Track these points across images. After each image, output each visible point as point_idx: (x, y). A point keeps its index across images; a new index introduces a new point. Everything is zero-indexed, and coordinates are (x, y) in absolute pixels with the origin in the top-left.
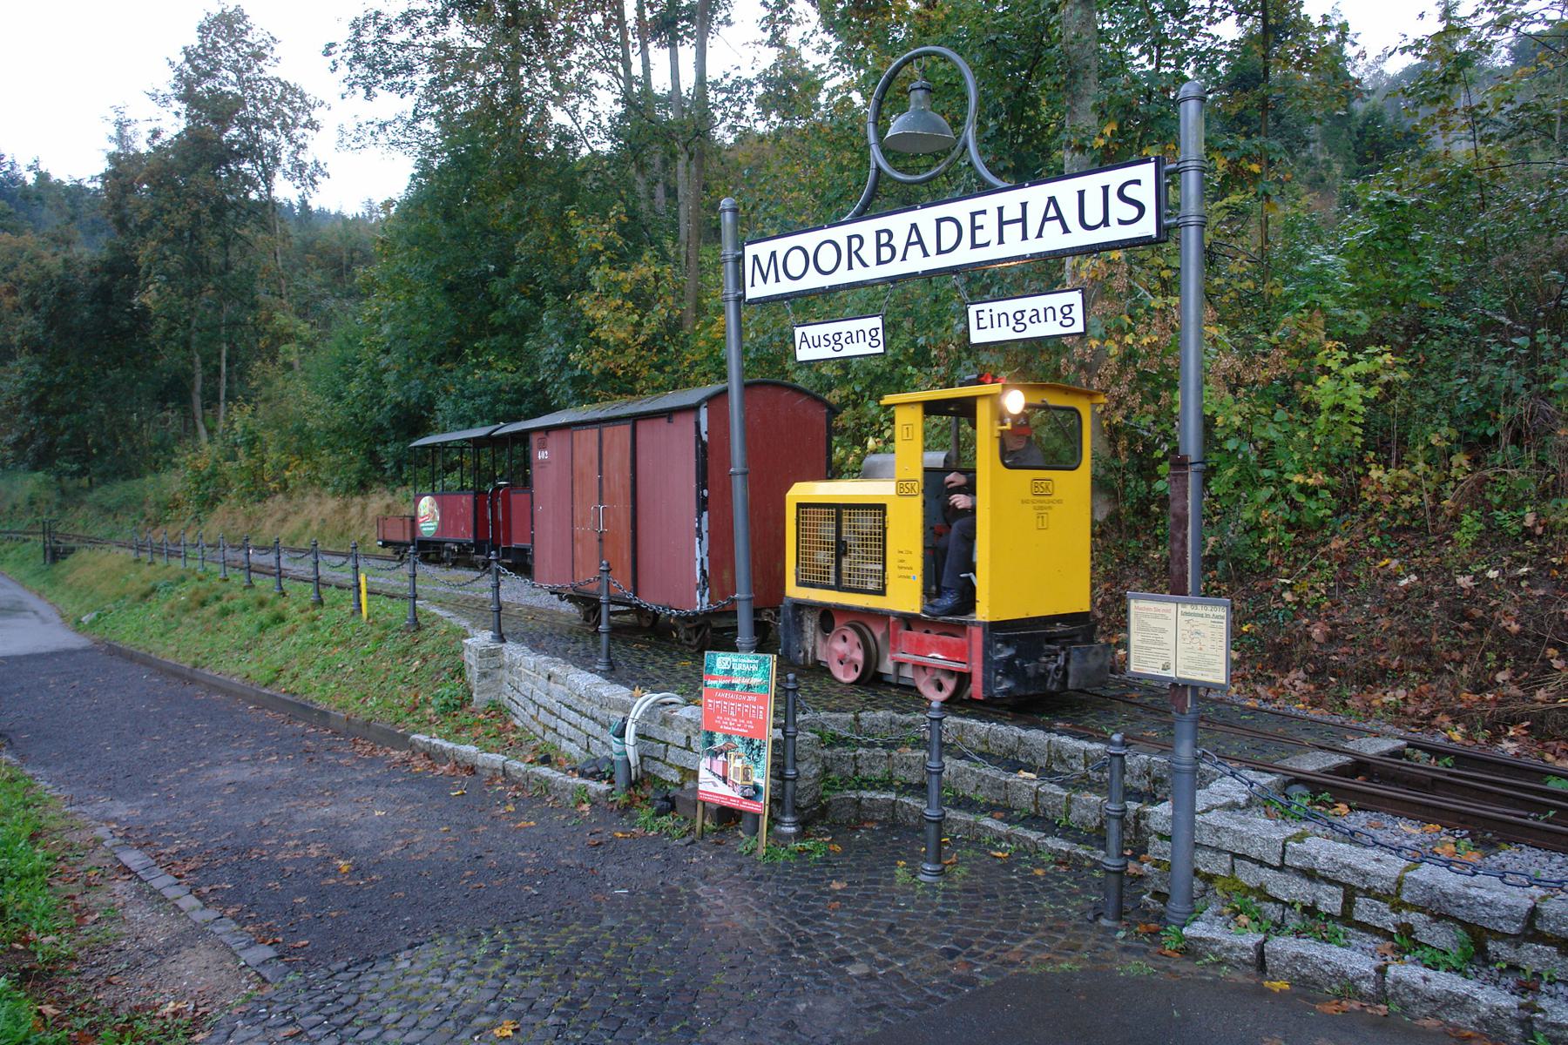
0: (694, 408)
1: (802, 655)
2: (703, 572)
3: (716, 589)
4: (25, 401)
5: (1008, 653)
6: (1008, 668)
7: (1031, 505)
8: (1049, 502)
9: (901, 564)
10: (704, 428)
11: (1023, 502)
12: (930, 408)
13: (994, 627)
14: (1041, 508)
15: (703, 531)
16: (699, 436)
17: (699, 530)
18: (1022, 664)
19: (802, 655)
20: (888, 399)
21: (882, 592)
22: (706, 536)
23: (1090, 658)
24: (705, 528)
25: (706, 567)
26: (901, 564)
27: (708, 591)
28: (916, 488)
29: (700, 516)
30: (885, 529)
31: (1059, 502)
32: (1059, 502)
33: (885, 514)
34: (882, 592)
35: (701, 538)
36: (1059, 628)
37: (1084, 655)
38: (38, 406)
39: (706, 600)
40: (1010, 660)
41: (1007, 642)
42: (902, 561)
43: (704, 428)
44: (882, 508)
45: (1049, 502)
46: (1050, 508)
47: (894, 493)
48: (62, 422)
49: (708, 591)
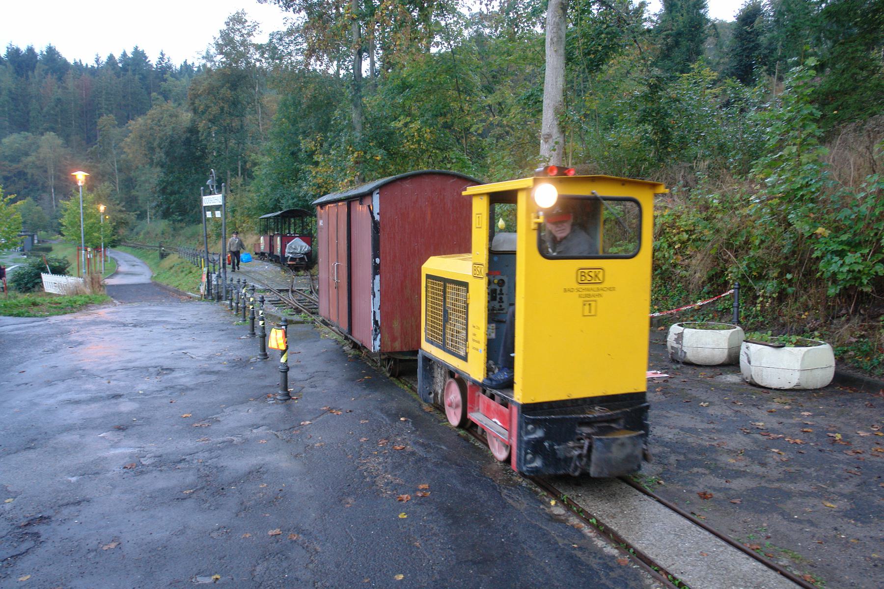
0: (370, 194)
1: (432, 395)
2: (376, 322)
3: (386, 336)
4: (158, 189)
5: (539, 434)
6: (536, 447)
8: (598, 289)
9: (475, 338)
10: (376, 210)
11: (565, 290)
13: (527, 409)
15: (376, 290)
16: (373, 217)
17: (373, 288)
18: (551, 446)
19: (432, 395)
21: (465, 358)
22: (378, 294)
23: (614, 449)
24: (377, 287)
25: (378, 318)
27: (379, 336)
29: (374, 279)
30: (468, 305)
31: (612, 289)
32: (612, 289)
33: (468, 292)
34: (465, 358)
35: (374, 296)
36: (597, 412)
37: (607, 446)
38: (163, 191)
39: (378, 343)
40: (539, 442)
41: (537, 424)
42: (474, 335)
43: (376, 210)
44: (465, 285)
45: (598, 289)
46: (600, 295)
48: (172, 198)
49: (379, 336)
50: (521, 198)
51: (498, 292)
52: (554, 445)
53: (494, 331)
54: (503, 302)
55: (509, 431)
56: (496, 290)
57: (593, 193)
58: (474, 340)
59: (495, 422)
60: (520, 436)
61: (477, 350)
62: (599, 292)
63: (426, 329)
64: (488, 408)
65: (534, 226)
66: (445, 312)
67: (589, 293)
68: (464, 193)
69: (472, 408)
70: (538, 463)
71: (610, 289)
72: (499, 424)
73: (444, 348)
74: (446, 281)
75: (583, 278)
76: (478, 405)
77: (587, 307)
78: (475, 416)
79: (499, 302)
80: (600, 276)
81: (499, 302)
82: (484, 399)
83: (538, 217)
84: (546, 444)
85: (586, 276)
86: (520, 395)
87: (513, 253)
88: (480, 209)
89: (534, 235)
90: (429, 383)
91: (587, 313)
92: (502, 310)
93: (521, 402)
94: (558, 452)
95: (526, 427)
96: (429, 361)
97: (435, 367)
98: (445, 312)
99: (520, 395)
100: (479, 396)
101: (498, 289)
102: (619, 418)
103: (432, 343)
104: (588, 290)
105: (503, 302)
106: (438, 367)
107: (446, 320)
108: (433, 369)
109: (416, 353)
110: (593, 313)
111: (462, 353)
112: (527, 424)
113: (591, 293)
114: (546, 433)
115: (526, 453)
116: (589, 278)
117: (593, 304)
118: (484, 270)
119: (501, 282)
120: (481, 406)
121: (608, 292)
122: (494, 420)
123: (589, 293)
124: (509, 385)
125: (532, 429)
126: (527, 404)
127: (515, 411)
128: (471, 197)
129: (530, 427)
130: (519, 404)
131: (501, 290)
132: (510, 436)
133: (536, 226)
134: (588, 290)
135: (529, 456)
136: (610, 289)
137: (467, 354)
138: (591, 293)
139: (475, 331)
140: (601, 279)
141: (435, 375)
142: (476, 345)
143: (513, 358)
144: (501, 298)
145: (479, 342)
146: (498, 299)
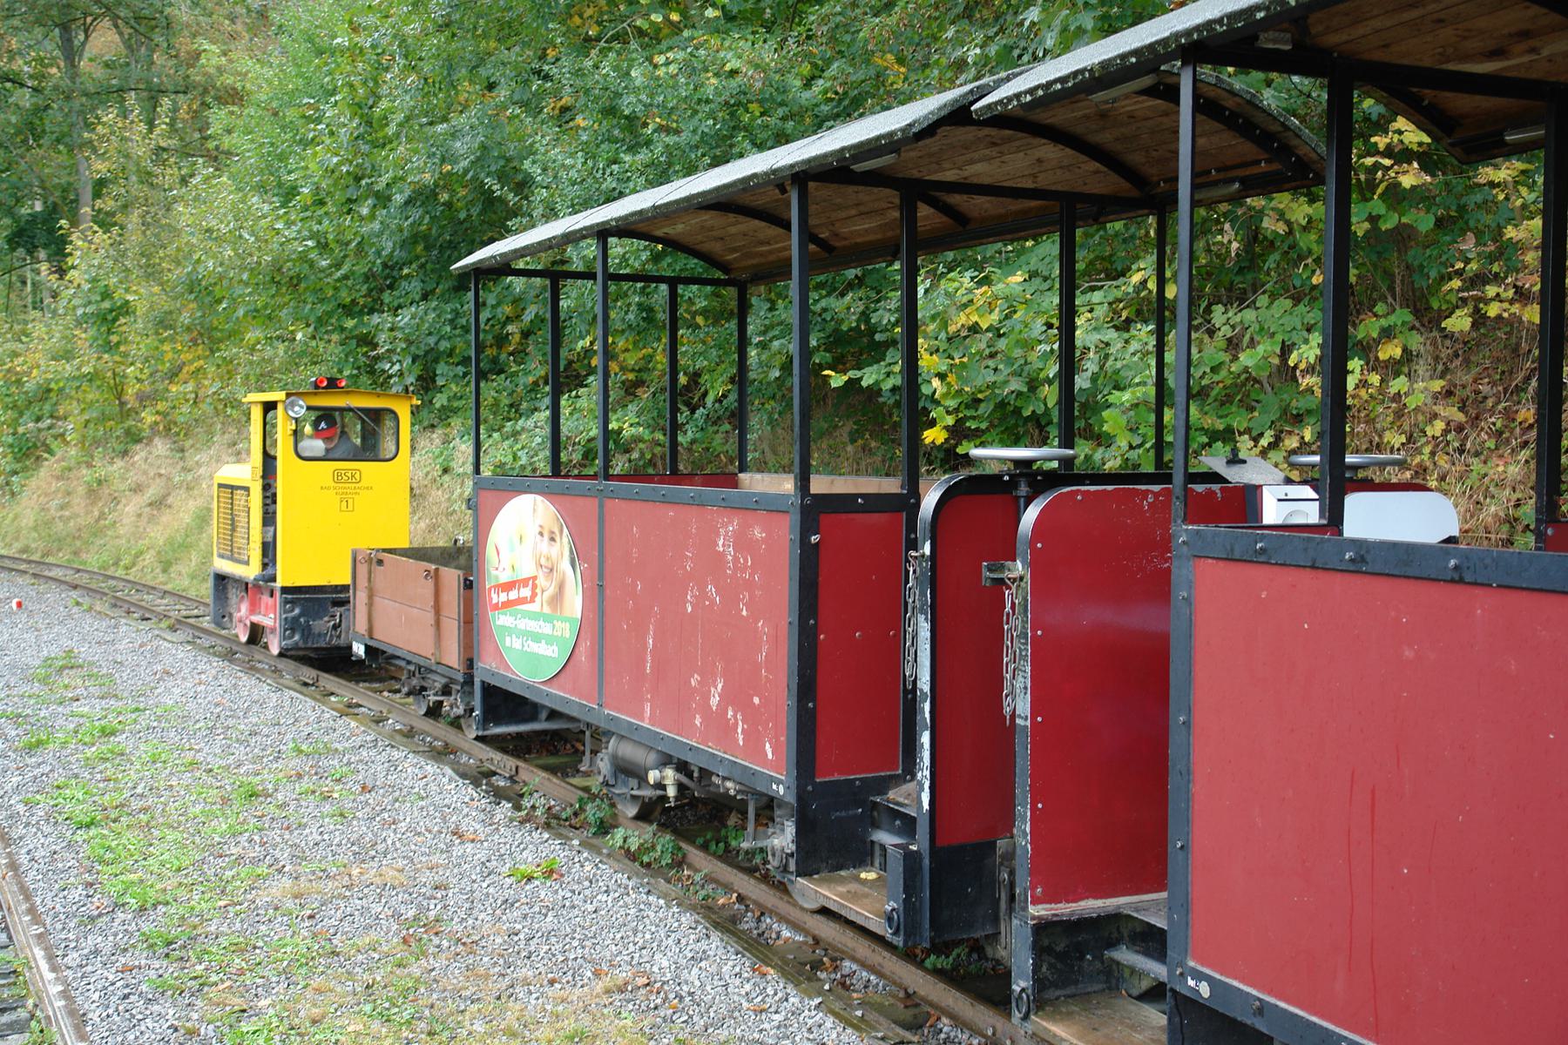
7: (334, 492)
21: (247, 563)
34: (247, 563)
44: (247, 489)
63: (218, 543)
65: (290, 432)
73: (232, 558)
74: (233, 488)
75: (338, 477)
77: (344, 503)
80: (357, 476)
97: (230, 587)
98: (233, 520)
103: (221, 556)
107: (233, 529)
110: (350, 508)
115: (285, 630)
117: (350, 501)
127: (278, 594)
141: (230, 595)
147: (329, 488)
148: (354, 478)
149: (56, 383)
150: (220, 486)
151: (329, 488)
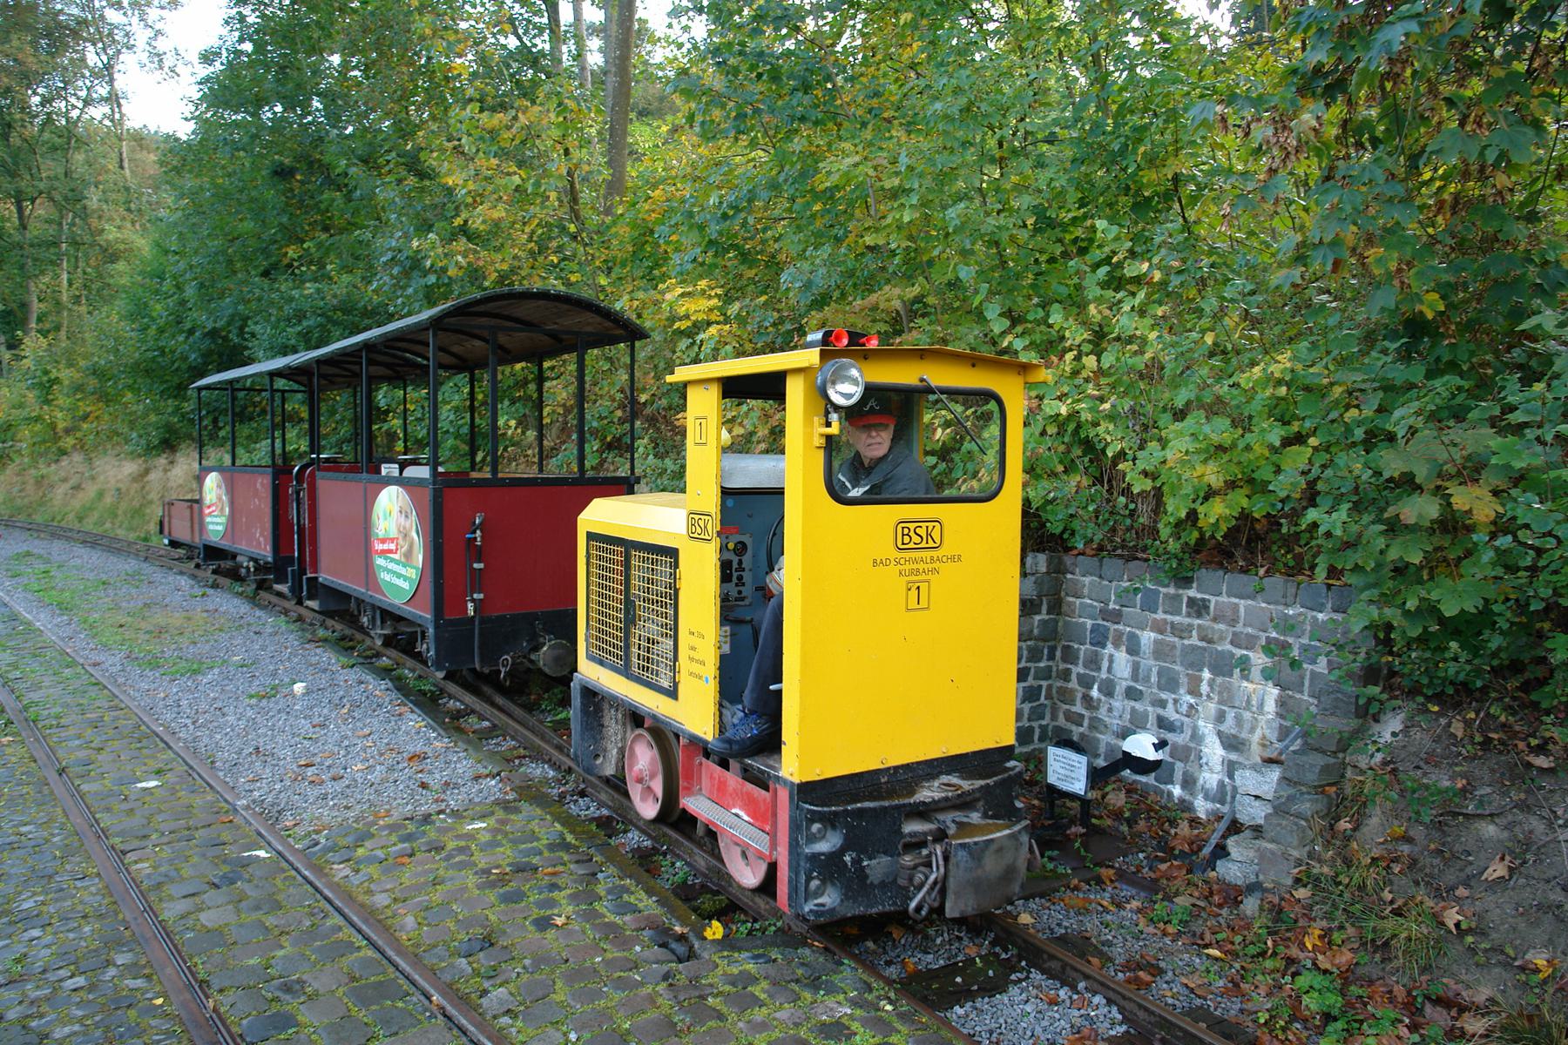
6: (829, 867)
7: (894, 569)
9: (692, 654)
12: (734, 388)
13: (807, 791)
14: (912, 572)
18: (857, 861)
20: (682, 374)
21: (673, 693)
26: (692, 654)
28: (709, 527)
30: (677, 591)
33: (677, 566)
34: (673, 693)
40: (835, 857)
41: (830, 821)
42: (693, 648)
44: (672, 553)
46: (937, 571)
47: (685, 532)
50: (795, 391)
51: (735, 565)
52: (862, 860)
53: (728, 639)
54: (743, 584)
55: (773, 835)
56: (730, 562)
57: (922, 380)
58: (691, 659)
59: (737, 815)
60: (794, 846)
61: (700, 678)
62: (934, 565)
64: (722, 786)
66: (629, 605)
67: (915, 566)
68: (669, 379)
69: (687, 789)
70: (829, 898)
71: (952, 559)
72: (746, 818)
73: (626, 672)
74: (628, 546)
75: (907, 539)
76: (700, 782)
78: (697, 804)
79: (737, 585)
81: (737, 585)
82: (711, 768)
83: (828, 424)
84: (847, 858)
85: (912, 534)
86: (793, 765)
87: (779, 492)
88: (703, 408)
89: (819, 458)
90: (594, 738)
91: (913, 604)
92: (743, 599)
93: (796, 780)
94: (867, 871)
95: (808, 828)
96: (594, 697)
97: (606, 706)
98: (629, 605)
99: (793, 765)
100: (701, 764)
101: (735, 560)
102: (978, 800)
104: (916, 561)
105: (743, 584)
106: (611, 706)
107: (630, 620)
108: (602, 711)
109: (566, 680)
110: (923, 604)
111: (666, 684)
112: (812, 821)
113: (921, 566)
114: (846, 838)
116: (917, 539)
117: (923, 587)
118: (714, 525)
119: (739, 546)
120: (705, 781)
121: (950, 564)
122: (734, 811)
123: (915, 566)
124: (770, 742)
125: (819, 830)
126: (807, 783)
127: (783, 795)
128: (682, 389)
129: (816, 827)
130: (792, 783)
131: (740, 562)
132: (773, 845)
133: (823, 441)
134: (916, 561)
135: (814, 884)
136: (952, 559)
137: (676, 684)
138: (921, 566)
139: (695, 641)
140: (938, 541)
141: (606, 721)
142: (696, 668)
143: (779, 693)
144: (740, 578)
145: (703, 663)
146: (735, 575)
147: (885, 563)
148: (928, 542)
149: (465, 257)
150: (591, 536)
151: (885, 563)
